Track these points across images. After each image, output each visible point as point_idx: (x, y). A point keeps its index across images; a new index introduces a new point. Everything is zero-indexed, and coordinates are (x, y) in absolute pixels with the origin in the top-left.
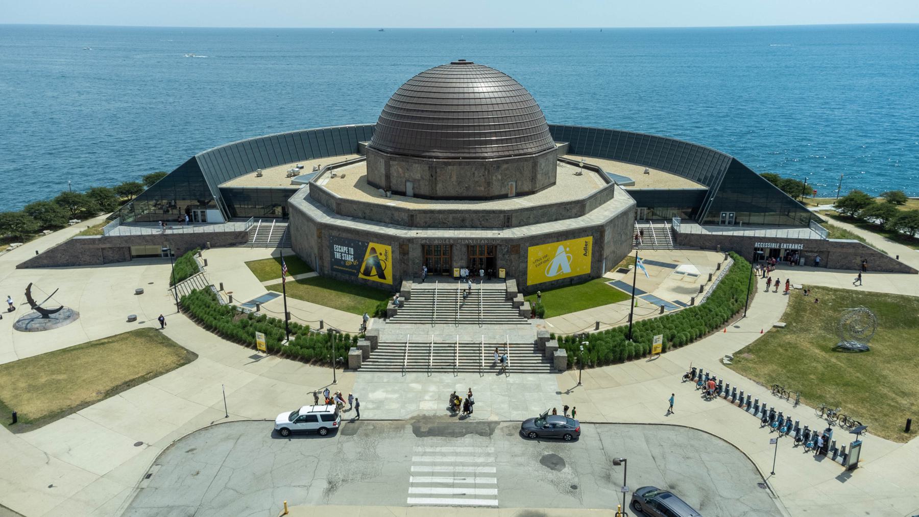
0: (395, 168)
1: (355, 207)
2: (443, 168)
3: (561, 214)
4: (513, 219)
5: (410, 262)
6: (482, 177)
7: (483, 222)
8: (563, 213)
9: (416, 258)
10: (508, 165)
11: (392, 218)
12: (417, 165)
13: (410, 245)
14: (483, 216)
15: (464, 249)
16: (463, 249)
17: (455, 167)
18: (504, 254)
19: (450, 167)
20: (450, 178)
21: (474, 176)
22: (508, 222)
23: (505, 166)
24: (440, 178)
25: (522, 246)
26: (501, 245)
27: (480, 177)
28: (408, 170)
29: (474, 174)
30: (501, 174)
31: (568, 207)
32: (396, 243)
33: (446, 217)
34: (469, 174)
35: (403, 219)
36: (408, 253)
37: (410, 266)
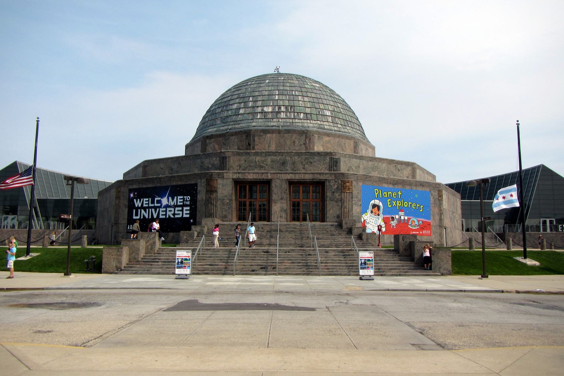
0: (212, 145)
1: (162, 165)
2: (261, 136)
3: (392, 172)
4: (342, 164)
5: (219, 203)
6: (303, 146)
7: (306, 166)
8: (395, 172)
9: (226, 196)
10: (330, 138)
11: (201, 166)
12: (234, 137)
13: (220, 181)
14: (307, 159)
15: (285, 186)
16: (283, 186)
17: (274, 135)
18: (333, 192)
19: (269, 135)
20: (269, 146)
21: (294, 145)
22: (336, 166)
23: (326, 139)
24: (258, 147)
25: (354, 183)
26: (329, 181)
27: (301, 145)
28: (224, 144)
29: (294, 142)
30: (323, 146)
31: (399, 166)
32: (203, 180)
33: (263, 159)
34: (288, 142)
35: (213, 165)
36: (216, 191)
37: (218, 206)
